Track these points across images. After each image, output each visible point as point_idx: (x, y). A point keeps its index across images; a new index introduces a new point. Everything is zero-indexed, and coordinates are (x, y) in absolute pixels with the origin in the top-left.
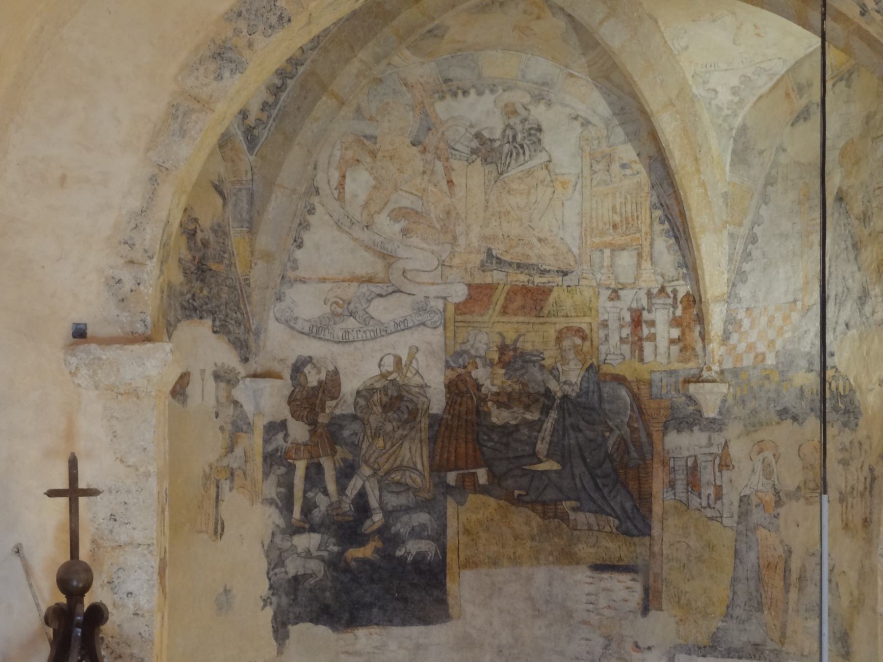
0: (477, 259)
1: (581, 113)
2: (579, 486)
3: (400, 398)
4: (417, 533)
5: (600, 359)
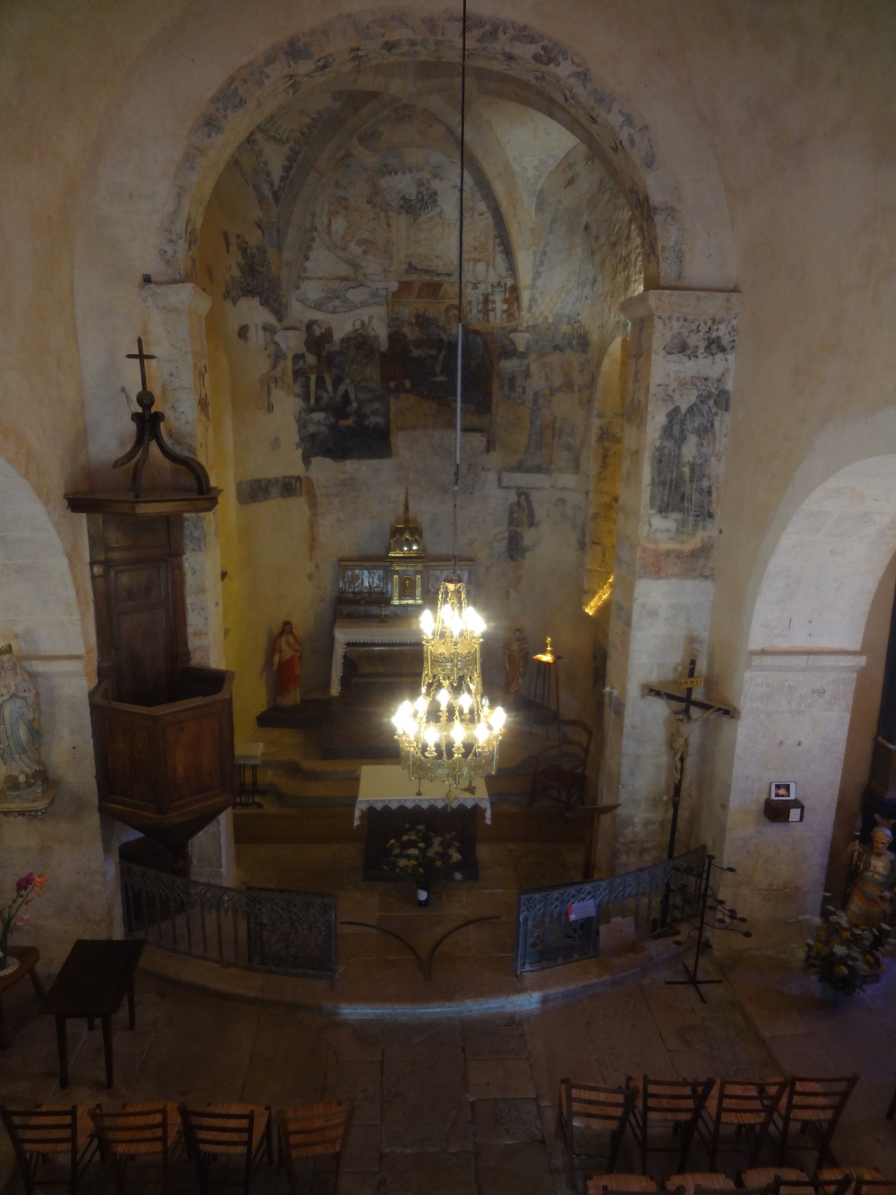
4: (375, 413)
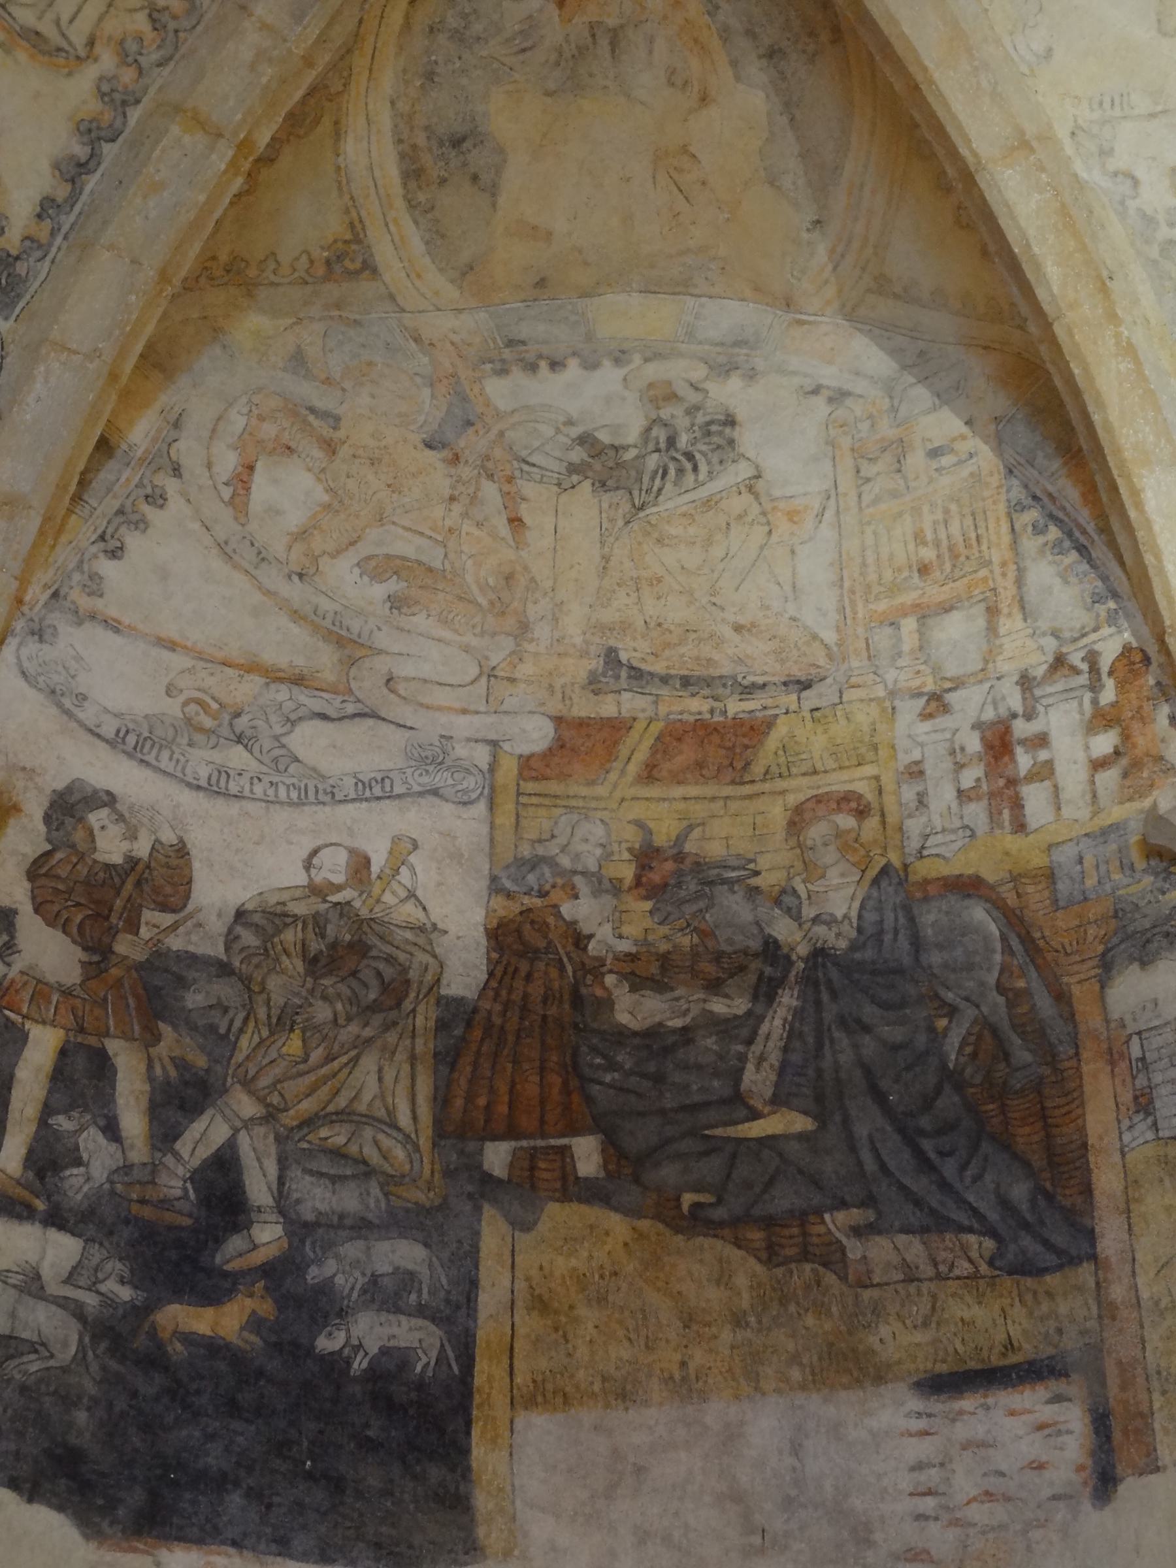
0: (579, 669)
1: (825, 382)
2: (870, 1165)
3: (359, 948)
5: (907, 850)
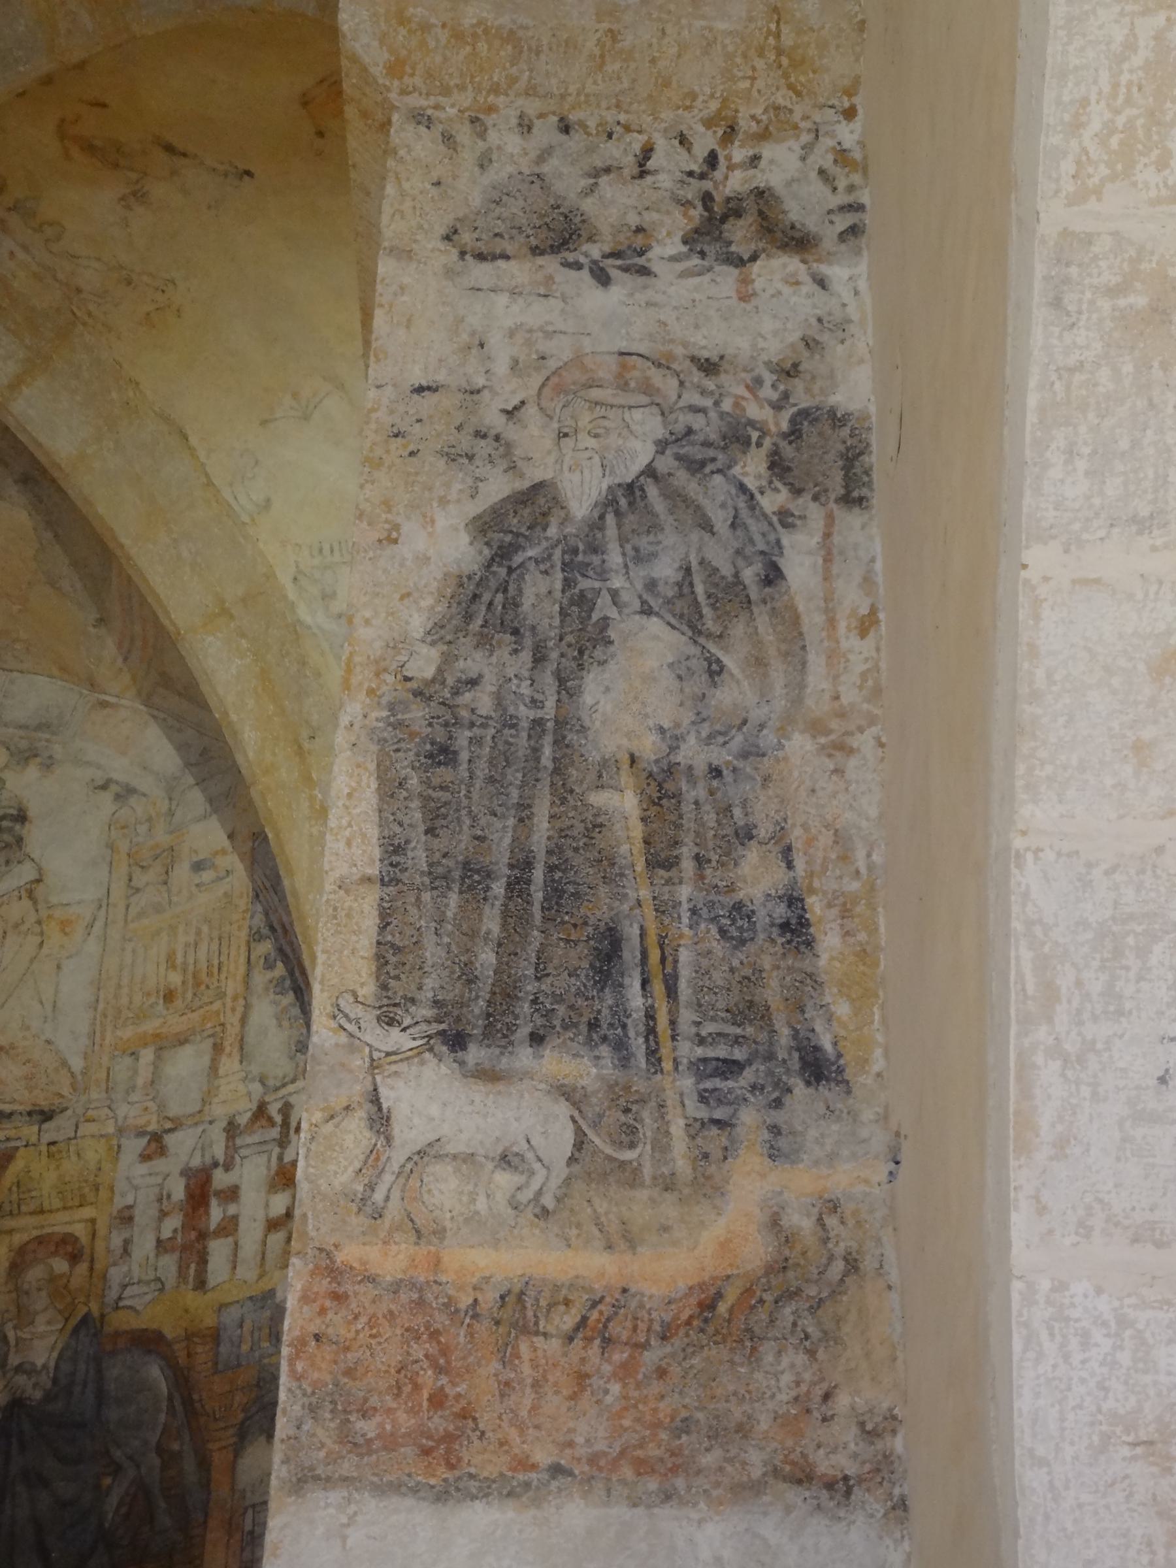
1: (115, 776)
5: (107, 1300)
